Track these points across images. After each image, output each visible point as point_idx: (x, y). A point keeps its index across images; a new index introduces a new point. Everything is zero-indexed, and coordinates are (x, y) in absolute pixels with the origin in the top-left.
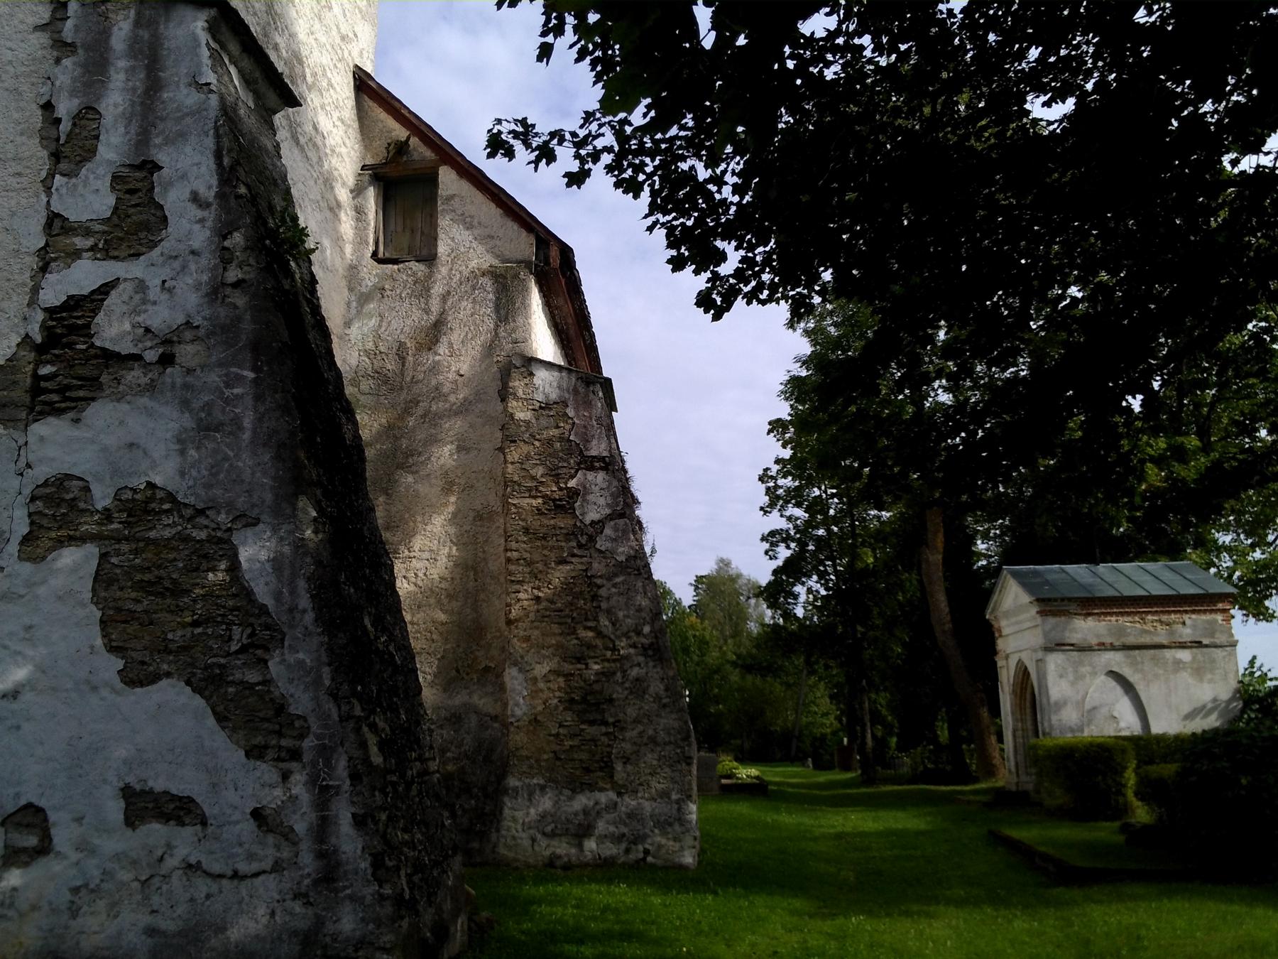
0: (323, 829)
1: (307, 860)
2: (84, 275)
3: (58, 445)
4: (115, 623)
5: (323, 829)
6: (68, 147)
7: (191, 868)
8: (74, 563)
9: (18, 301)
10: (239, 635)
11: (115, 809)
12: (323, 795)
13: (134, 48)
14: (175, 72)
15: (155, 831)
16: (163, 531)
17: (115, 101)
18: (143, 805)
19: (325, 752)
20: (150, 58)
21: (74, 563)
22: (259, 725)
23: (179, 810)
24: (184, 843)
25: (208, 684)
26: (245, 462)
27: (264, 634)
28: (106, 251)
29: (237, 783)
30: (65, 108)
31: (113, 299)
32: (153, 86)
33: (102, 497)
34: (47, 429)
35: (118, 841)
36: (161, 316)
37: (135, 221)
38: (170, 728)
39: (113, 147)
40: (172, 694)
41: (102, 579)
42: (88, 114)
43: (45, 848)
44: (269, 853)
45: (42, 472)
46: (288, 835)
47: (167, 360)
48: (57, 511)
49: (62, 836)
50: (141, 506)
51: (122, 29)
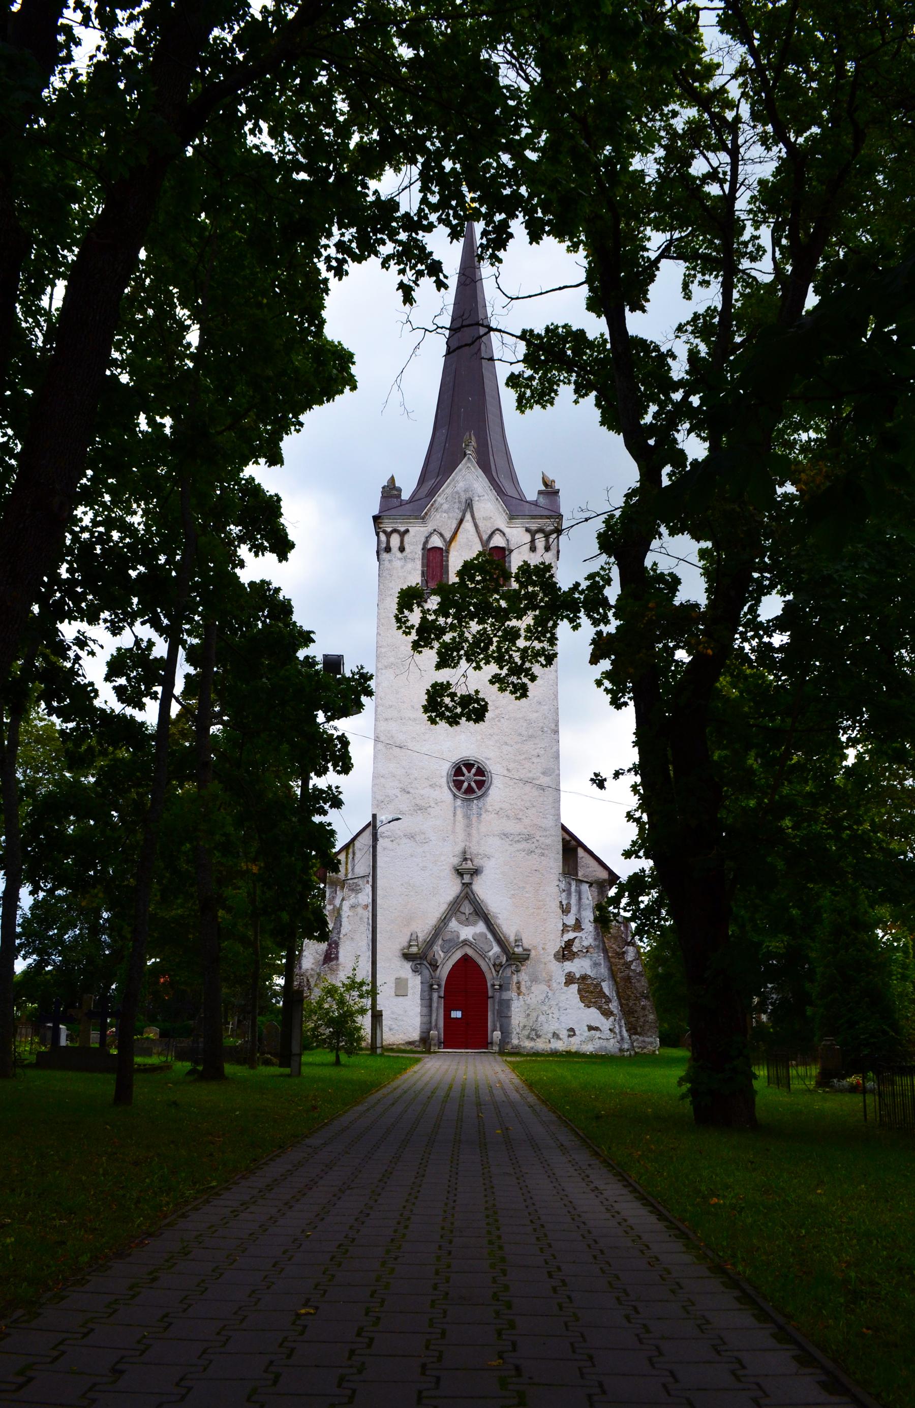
0: (621, 1032)
1: (619, 1037)
2: (571, 935)
3: (569, 966)
4: (582, 999)
5: (621, 1032)
6: (566, 910)
7: (599, 1038)
8: (574, 987)
9: (558, 940)
10: (604, 1000)
11: (586, 1028)
12: (620, 1027)
13: (576, 891)
14: (584, 896)
15: (593, 1032)
16: (589, 981)
17: (573, 901)
18: (590, 1028)
19: (620, 1020)
20: (579, 893)
21: (574, 987)
22: (607, 1014)
23: (597, 1029)
24: (598, 1034)
25: (599, 1008)
26: (603, 970)
27: (609, 1001)
28: (574, 931)
29: (606, 1024)
30: (564, 903)
31: (576, 940)
32: (580, 899)
33: (578, 976)
34: (567, 963)
35: (587, 1034)
36: (586, 943)
37: (578, 926)
38: (593, 1016)
39: (574, 909)
40: (593, 1010)
41: (579, 991)
42: (569, 904)
43: (575, 1035)
44: (612, 1035)
45: (566, 971)
46: (615, 1033)
47: (587, 952)
48: (570, 979)
49: (577, 1033)
50: (584, 978)
51: (573, 888)
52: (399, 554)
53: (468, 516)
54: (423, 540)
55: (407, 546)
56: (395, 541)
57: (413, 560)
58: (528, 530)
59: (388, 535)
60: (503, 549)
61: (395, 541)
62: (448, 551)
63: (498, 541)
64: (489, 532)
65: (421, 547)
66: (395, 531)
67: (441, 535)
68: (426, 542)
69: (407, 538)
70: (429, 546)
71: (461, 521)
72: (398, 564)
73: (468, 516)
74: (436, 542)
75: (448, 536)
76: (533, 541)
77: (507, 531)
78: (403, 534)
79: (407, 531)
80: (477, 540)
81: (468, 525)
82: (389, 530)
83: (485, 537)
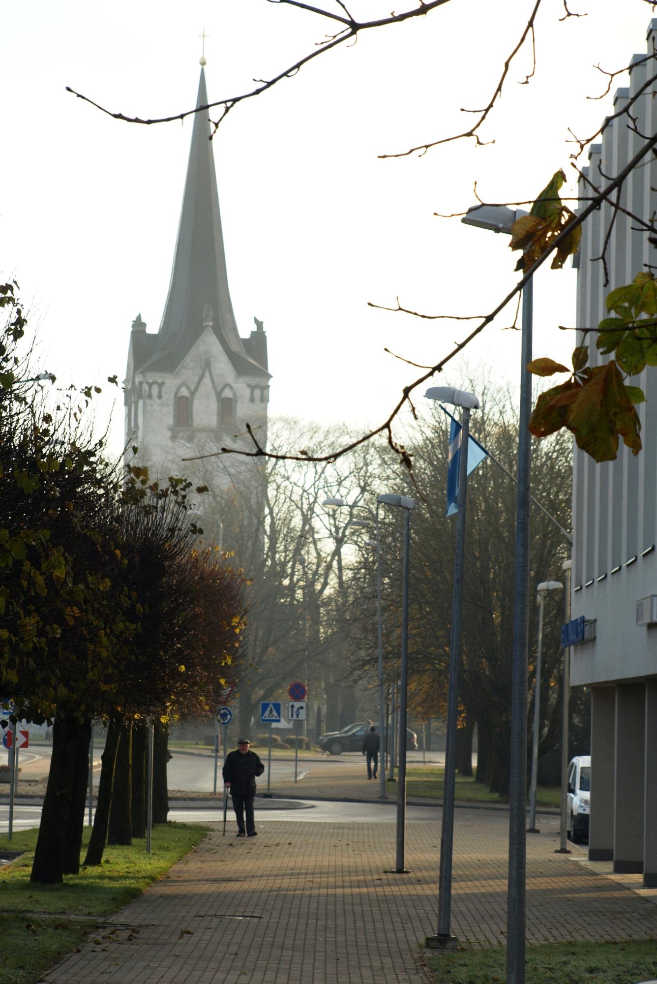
52: (157, 401)
53: (207, 374)
54: (174, 390)
55: (163, 394)
56: (155, 390)
57: (168, 405)
58: (249, 386)
59: (150, 385)
60: (230, 399)
61: (155, 390)
62: (192, 400)
63: (227, 393)
64: (221, 386)
65: (173, 395)
66: (155, 382)
67: (188, 388)
68: (177, 393)
69: (164, 389)
70: (179, 395)
71: (202, 377)
72: (157, 408)
73: (207, 374)
74: (184, 392)
75: (192, 388)
76: (252, 394)
77: (234, 385)
78: (161, 385)
79: (163, 383)
80: (213, 392)
81: (207, 380)
82: (150, 381)
83: (218, 390)
